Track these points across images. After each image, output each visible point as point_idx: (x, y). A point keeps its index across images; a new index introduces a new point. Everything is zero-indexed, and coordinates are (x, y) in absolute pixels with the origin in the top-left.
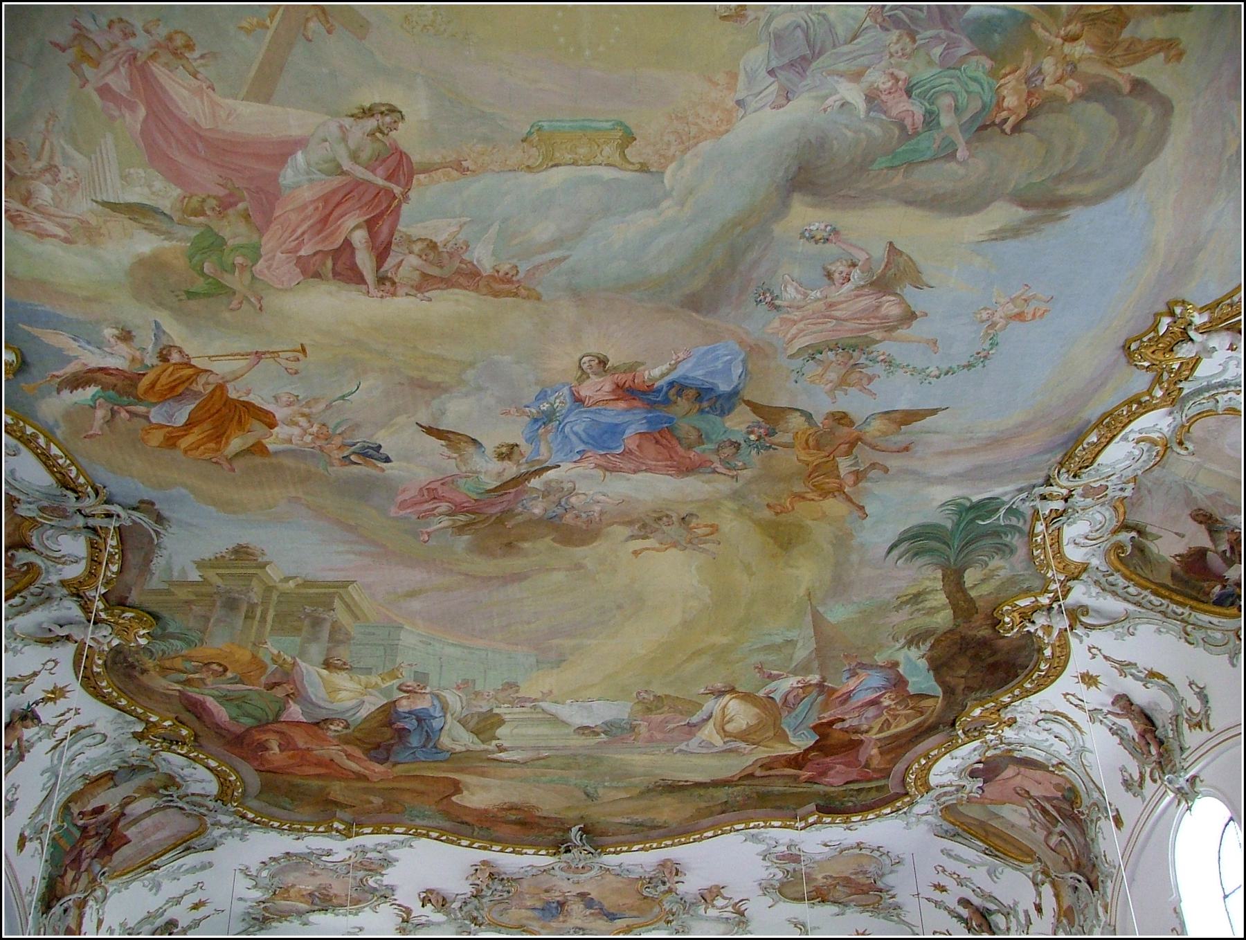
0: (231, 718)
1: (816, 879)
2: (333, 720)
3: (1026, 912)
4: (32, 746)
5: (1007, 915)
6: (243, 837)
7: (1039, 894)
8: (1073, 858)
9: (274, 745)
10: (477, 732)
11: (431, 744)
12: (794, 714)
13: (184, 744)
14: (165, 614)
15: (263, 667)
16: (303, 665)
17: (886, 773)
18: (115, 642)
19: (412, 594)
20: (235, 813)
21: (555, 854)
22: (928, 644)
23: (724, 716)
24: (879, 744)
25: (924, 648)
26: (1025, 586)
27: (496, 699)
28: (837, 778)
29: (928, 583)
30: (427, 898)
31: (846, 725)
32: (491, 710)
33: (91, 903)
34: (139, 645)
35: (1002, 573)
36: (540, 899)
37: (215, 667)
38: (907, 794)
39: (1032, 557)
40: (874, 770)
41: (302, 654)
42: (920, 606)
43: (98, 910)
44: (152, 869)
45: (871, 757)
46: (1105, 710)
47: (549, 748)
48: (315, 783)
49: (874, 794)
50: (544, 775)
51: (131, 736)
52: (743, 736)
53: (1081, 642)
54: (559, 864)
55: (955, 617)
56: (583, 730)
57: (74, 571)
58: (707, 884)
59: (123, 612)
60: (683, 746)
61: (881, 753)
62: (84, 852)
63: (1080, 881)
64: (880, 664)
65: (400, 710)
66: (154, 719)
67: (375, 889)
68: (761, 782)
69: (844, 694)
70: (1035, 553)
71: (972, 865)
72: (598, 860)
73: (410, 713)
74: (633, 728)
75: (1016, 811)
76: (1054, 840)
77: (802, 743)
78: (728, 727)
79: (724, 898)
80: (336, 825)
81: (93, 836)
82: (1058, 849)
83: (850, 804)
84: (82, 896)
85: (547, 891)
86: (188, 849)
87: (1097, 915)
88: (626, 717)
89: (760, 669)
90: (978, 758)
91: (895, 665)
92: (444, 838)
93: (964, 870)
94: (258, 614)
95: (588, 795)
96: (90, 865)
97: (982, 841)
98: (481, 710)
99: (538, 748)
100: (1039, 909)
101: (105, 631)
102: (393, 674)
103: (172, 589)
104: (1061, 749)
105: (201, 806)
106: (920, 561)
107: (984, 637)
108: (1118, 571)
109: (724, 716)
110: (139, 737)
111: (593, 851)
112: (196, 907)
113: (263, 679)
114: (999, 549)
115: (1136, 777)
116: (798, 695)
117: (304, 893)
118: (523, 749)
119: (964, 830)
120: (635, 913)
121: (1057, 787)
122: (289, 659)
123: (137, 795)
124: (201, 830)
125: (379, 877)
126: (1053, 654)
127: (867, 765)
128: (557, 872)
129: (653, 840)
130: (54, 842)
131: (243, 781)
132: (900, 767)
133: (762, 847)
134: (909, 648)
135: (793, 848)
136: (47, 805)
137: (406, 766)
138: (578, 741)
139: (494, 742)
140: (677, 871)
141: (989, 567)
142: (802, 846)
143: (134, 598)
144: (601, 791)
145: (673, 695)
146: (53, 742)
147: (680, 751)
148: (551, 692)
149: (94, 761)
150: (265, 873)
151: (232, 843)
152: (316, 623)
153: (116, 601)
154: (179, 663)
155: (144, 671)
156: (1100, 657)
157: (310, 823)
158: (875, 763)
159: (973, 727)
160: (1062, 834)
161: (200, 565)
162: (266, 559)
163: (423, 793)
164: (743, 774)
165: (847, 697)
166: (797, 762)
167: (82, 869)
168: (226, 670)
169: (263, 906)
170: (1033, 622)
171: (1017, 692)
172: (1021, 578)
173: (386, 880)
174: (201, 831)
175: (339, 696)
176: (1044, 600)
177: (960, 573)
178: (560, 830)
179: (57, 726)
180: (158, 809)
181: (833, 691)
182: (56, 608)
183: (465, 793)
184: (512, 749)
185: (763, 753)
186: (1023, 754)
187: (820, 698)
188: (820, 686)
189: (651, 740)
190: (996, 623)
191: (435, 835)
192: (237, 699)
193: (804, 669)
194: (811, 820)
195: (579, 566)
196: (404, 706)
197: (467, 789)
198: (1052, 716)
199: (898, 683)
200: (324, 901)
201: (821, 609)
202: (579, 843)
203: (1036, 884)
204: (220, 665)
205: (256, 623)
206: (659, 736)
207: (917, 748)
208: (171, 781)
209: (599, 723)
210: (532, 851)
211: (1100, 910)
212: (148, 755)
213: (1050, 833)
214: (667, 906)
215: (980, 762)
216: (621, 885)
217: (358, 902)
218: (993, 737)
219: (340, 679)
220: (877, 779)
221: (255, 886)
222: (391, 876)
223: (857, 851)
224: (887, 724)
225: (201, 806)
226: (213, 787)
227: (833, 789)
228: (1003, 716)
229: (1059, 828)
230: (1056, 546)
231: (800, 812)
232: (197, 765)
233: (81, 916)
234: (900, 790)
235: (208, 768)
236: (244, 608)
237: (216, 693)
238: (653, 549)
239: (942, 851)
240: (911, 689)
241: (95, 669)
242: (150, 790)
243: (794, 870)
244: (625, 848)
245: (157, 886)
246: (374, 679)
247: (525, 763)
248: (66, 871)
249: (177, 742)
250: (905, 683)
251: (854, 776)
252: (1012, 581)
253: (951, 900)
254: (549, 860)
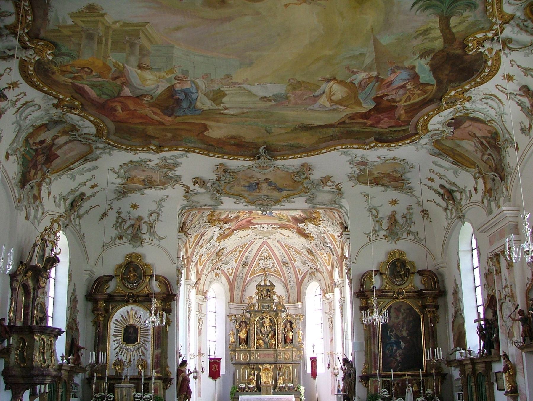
0: (97, 95)
1: (373, 174)
2: (146, 95)
3: (470, 191)
4: (6, 111)
5: (461, 193)
6: (110, 154)
7: (476, 183)
8: (494, 166)
9: (119, 108)
10: (214, 100)
11: (193, 106)
12: (364, 92)
13: (77, 109)
14: (59, 42)
15: (109, 69)
16: (128, 67)
17: (408, 123)
18: (37, 58)
19: (178, 29)
20: (105, 142)
21: (253, 160)
22: (430, 57)
23: (330, 92)
24: (405, 108)
25: (429, 59)
26: (481, 27)
27: (222, 83)
28: (384, 125)
29: (431, 24)
30: (196, 181)
31: (389, 98)
32: (220, 89)
33: (44, 184)
34: (48, 59)
35: (470, 19)
36: (248, 182)
37: (86, 70)
38: (417, 134)
39: (486, 11)
40: (403, 121)
41: (127, 61)
42: (428, 36)
43: (48, 188)
44: (71, 169)
45: (401, 115)
46: (515, 93)
47: (248, 108)
48: (140, 127)
49: (402, 133)
50: (246, 121)
51: (52, 106)
52: (340, 102)
53: (507, 57)
54: (255, 165)
55: (445, 42)
56: (264, 99)
57: (10, 20)
58: (324, 175)
59: (38, 42)
60: (311, 107)
61: (406, 113)
62: (38, 162)
63: (496, 176)
64: (406, 67)
65: (176, 89)
66: (61, 97)
67: (172, 177)
68: (349, 126)
69: (388, 82)
70: (488, 8)
71: (446, 169)
72: (272, 163)
73: (181, 91)
74: (287, 98)
75: (468, 143)
76: (485, 157)
77: (369, 106)
78: (333, 98)
79: (332, 182)
80: (151, 147)
81: (41, 154)
82: (487, 161)
83: (390, 138)
84: (39, 181)
85: (250, 178)
86: (86, 160)
87: (503, 192)
88: (283, 92)
89: (348, 68)
90: (452, 117)
91: (413, 68)
92: (201, 152)
93: (442, 171)
94: (104, 41)
95: (267, 131)
96: (41, 167)
97: (451, 158)
98: (215, 89)
99: (243, 108)
100: (476, 189)
101: (31, 52)
102: (171, 71)
103: (61, 29)
104: (492, 113)
105: (89, 139)
106: (428, 12)
107: (458, 54)
108: (529, 18)
109: (330, 92)
110: (56, 106)
111: (271, 158)
112: (93, 187)
113: (110, 76)
114: (469, 6)
115: (527, 126)
116: (366, 82)
117: (141, 180)
118: (235, 108)
119: (444, 153)
120: (291, 189)
121: (489, 131)
122: (121, 65)
123: (59, 135)
124: (91, 151)
125: (173, 172)
126: (492, 64)
127: (399, 118)
128: (255, 169)
129: (298, 153)
130: (23, 156)
131: (107, 127)
132: (415, 120)
133: (349, 158)
134: (421, 59)
135: (363, 158)
136: (17, 139)
137: (182, 118)
138: (261, 104)
139: (222, 105)
140: (310, 168)
141: (464, 16)
142: (367, 158)
143: (42, 34)
144: (273, 129)
145: (306, 81)
146: (15, 109)
147: (310, 109)
148: (247, 79)
149: (37, 118)
150: (122, 171)
151: (105, 157)
152: (132, 45)
153: (35, 36)
154: (69, 68)
155: (53, 73)
156: (515, 66)
157: (140, 146)
158: (403, 117)
159: (450, 101)
160: (489, 154)
161: (72, 15)
162: (104, 12)
163: (190, 131)
164: (340, 121)
165: (390, 84)
166: (365, 116)
167: (38, 169)
168: (92, 71)
169: (123, 186)
170: (483, 47)
171: (473, 83)
172: (479, 22)
173: (177, 173)
174: (91, 152)
175: (147, 83)
176: (490, 35)
177: (448, 19)
178: (255, 148)
179: (16, 101)
180: (70, 141)
181: (383, 80)
182: (5, 41)
183: (210, 130)
185: (349, 111)
186: (474, 115)
187: (377, 84)
188: (377, 77)
189: (296, 104)
190: (465, 46)
191: (197, 151)
192: (99, 86)
193: (369, 68)
194: (372, 145)
195: (258, 13)
196: (178, 87)
197: (211, 128)
198: (489, 97)
199: (415, 77)
200: (150, 184)
201: (378, 37)
202: (264, 155)
203: (475, 178)
204: (89, 69)
205: (103, 46)
206: (300, 102)
207: (422, 111)
208: (74, 128)
209: (271, 95)
210: (242, 159)
211: (504, 189)
212: (62, 115)
213: (484, 154)
214: (305, 185)
215: (452, 119)
216: (284, 175)
217: (165, 183)
218: (460, 106)
219: (147, 74)
220: (404, 126)
221: (118, 177)
222: (178, 171)
223: (393, 161)
224: (409, 98)
225: (89, 139)
226: (93, 130)
227: (382, 130)
228: (465, 95)
229: (489, 151)
230: (499, 4)
231: (367, 141)
232: (85, 120)
233: (40, 191)
234: (414, 132)
235: (90, 121)
236: (96, 39)
237: (88, 83)
238: (295, 4)
239: (433, 162)
240: (421, 81)
241: (30, 72)
242: (65, 132)
243: (364, 170)
244: (285, 157)
245: (73, 178)
246: (163, 74)
247: (237, 115)
248: (30, 170)
249: (74, 108)
250: (419, 77)
251: (393, 124)
252: (474, 24)
253: (436, 186)
254: (250, 163)
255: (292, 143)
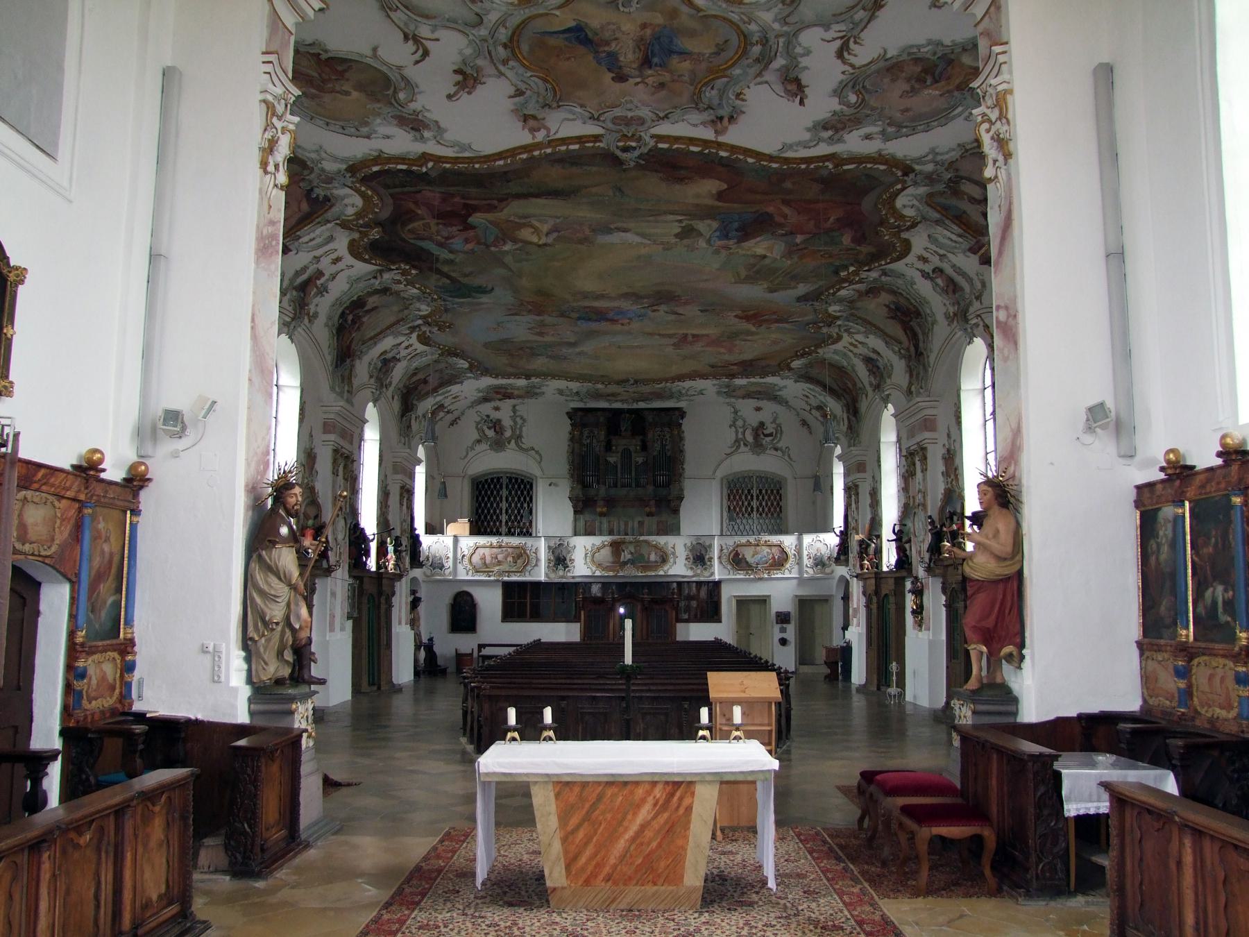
19: (706, 280)
56: (625, 231)
60: (558, 221)
85: (662, 85)
95: (620, 190)
118: (666, 222)
144: (611, 193)
147: (559, 218)
183: (714, 192)
184: (672, 221)
255: (575, 170)
